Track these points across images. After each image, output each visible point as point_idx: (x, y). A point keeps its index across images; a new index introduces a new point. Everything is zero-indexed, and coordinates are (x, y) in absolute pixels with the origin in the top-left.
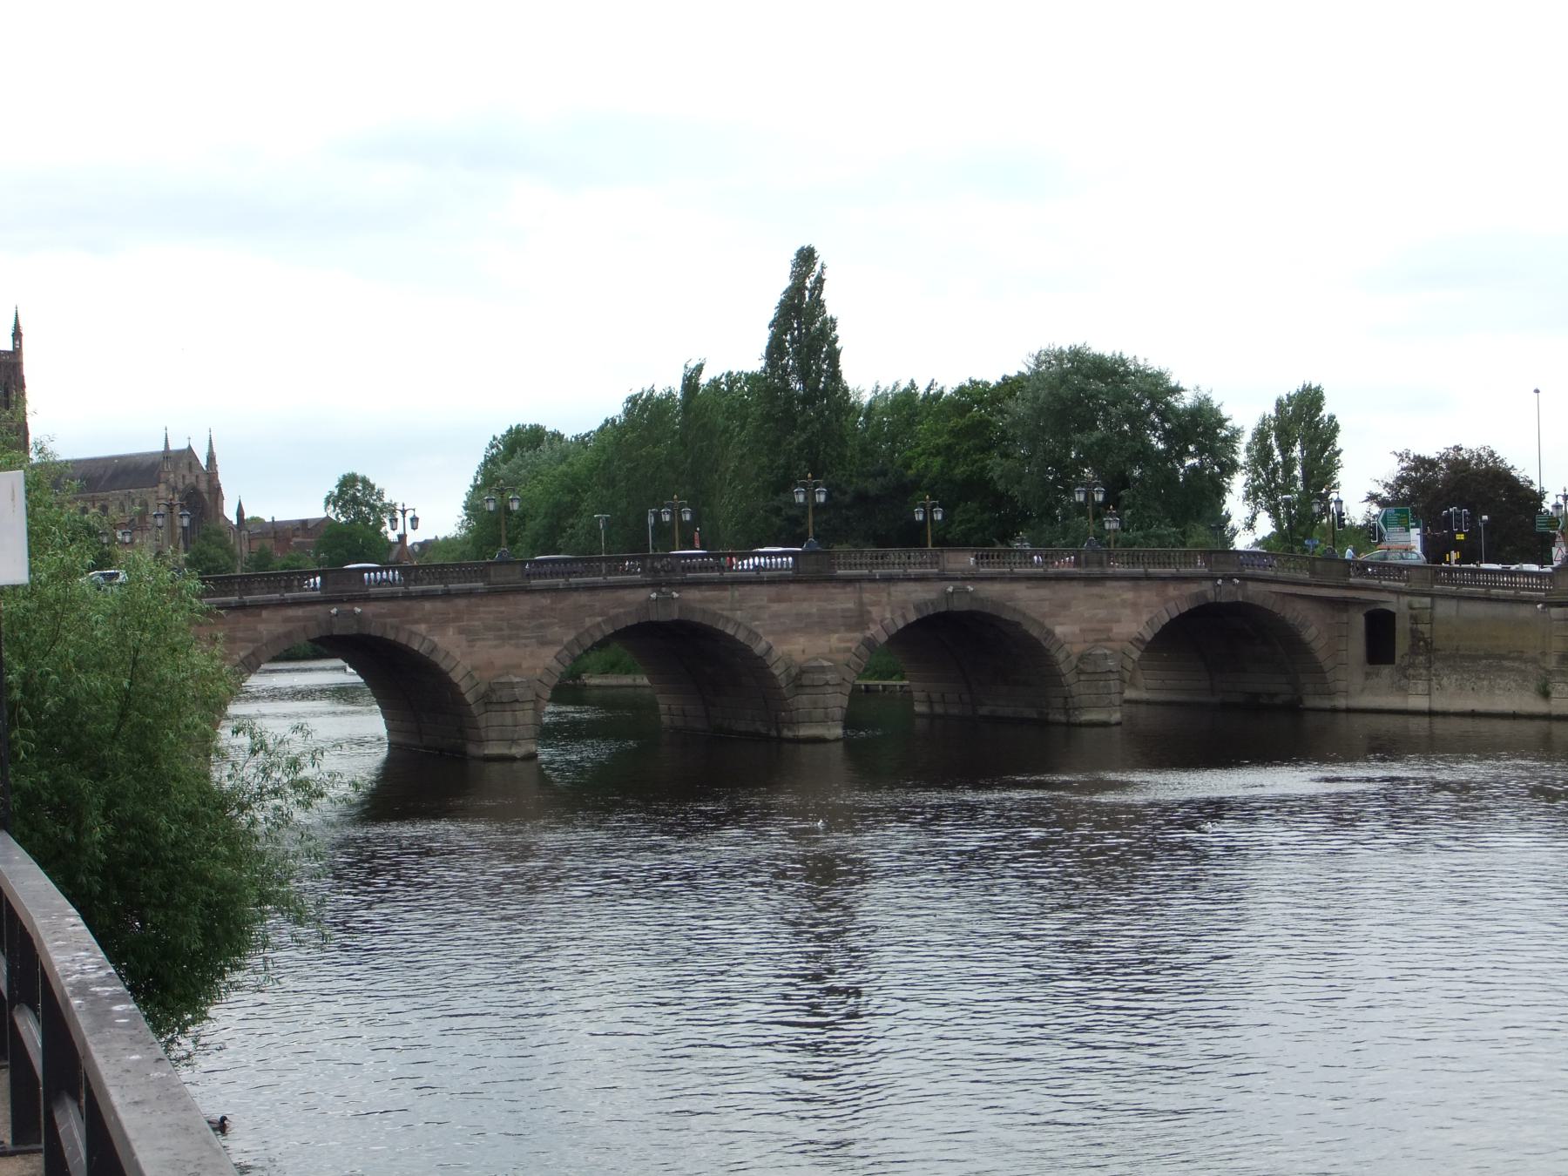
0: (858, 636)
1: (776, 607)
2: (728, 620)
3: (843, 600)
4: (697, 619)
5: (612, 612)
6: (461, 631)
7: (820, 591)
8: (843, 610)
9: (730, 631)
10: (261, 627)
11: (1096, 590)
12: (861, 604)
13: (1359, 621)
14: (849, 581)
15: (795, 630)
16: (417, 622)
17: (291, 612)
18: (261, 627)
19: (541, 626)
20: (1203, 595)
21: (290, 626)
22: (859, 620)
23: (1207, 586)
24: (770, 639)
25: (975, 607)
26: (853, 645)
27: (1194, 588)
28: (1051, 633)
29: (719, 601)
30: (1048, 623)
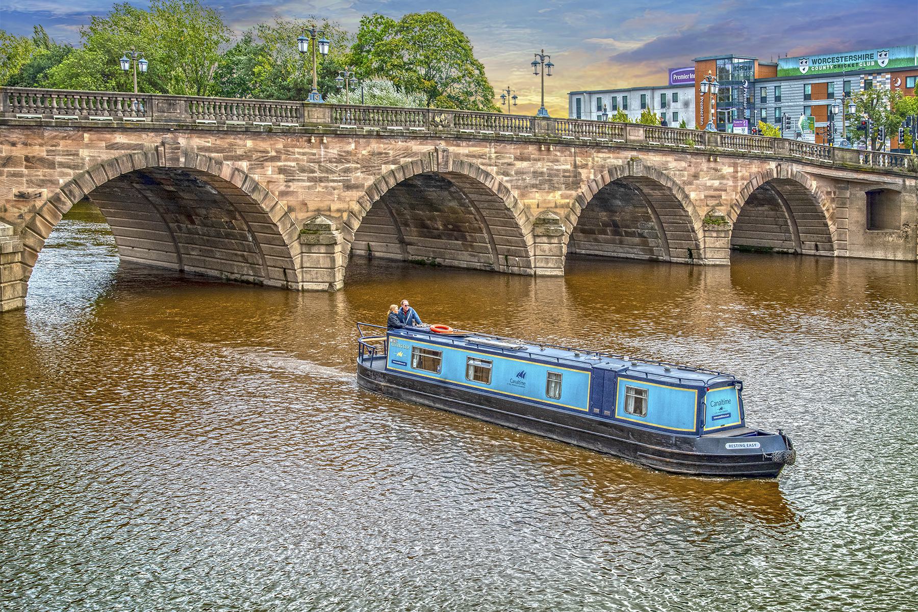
1: (520, 165)
3: (564, 162)
5: (403, 161)
6: (281, 171)
8: (565, 171)
10: (84, 153)
12: (576, 166)
13: (861, 194)
15: (533, 186)
16: (239, 158)
18: (84, 153)
21: (115, 153)
22: (574, 181)
26: (570, 201)
28: (687, 197)
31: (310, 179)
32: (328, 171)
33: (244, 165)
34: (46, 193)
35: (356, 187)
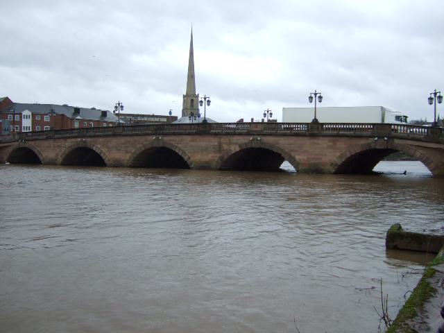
0: (218, 155)
1: (192, 144)
2: (176, 147)
3: (214, 142)
4: (168, 146)
5: (145, 143)
7: (206, 138)
9: (177, 151)
10: (67, 144)
11: (316, 141)
14: (216, 134)
17: (73, 140)
19: (126, 147)
20: (369, 145)
23: (370, 140)
24: (189, 155)
25: (263, 146)
26: (216, 159)
27: (363, 142)
29: (173, 141)
30: (293, 154)
31: (117, 150)
32: (121, 147)
33: (99, 146)
34: (60, 154)
35: (130, 152)
